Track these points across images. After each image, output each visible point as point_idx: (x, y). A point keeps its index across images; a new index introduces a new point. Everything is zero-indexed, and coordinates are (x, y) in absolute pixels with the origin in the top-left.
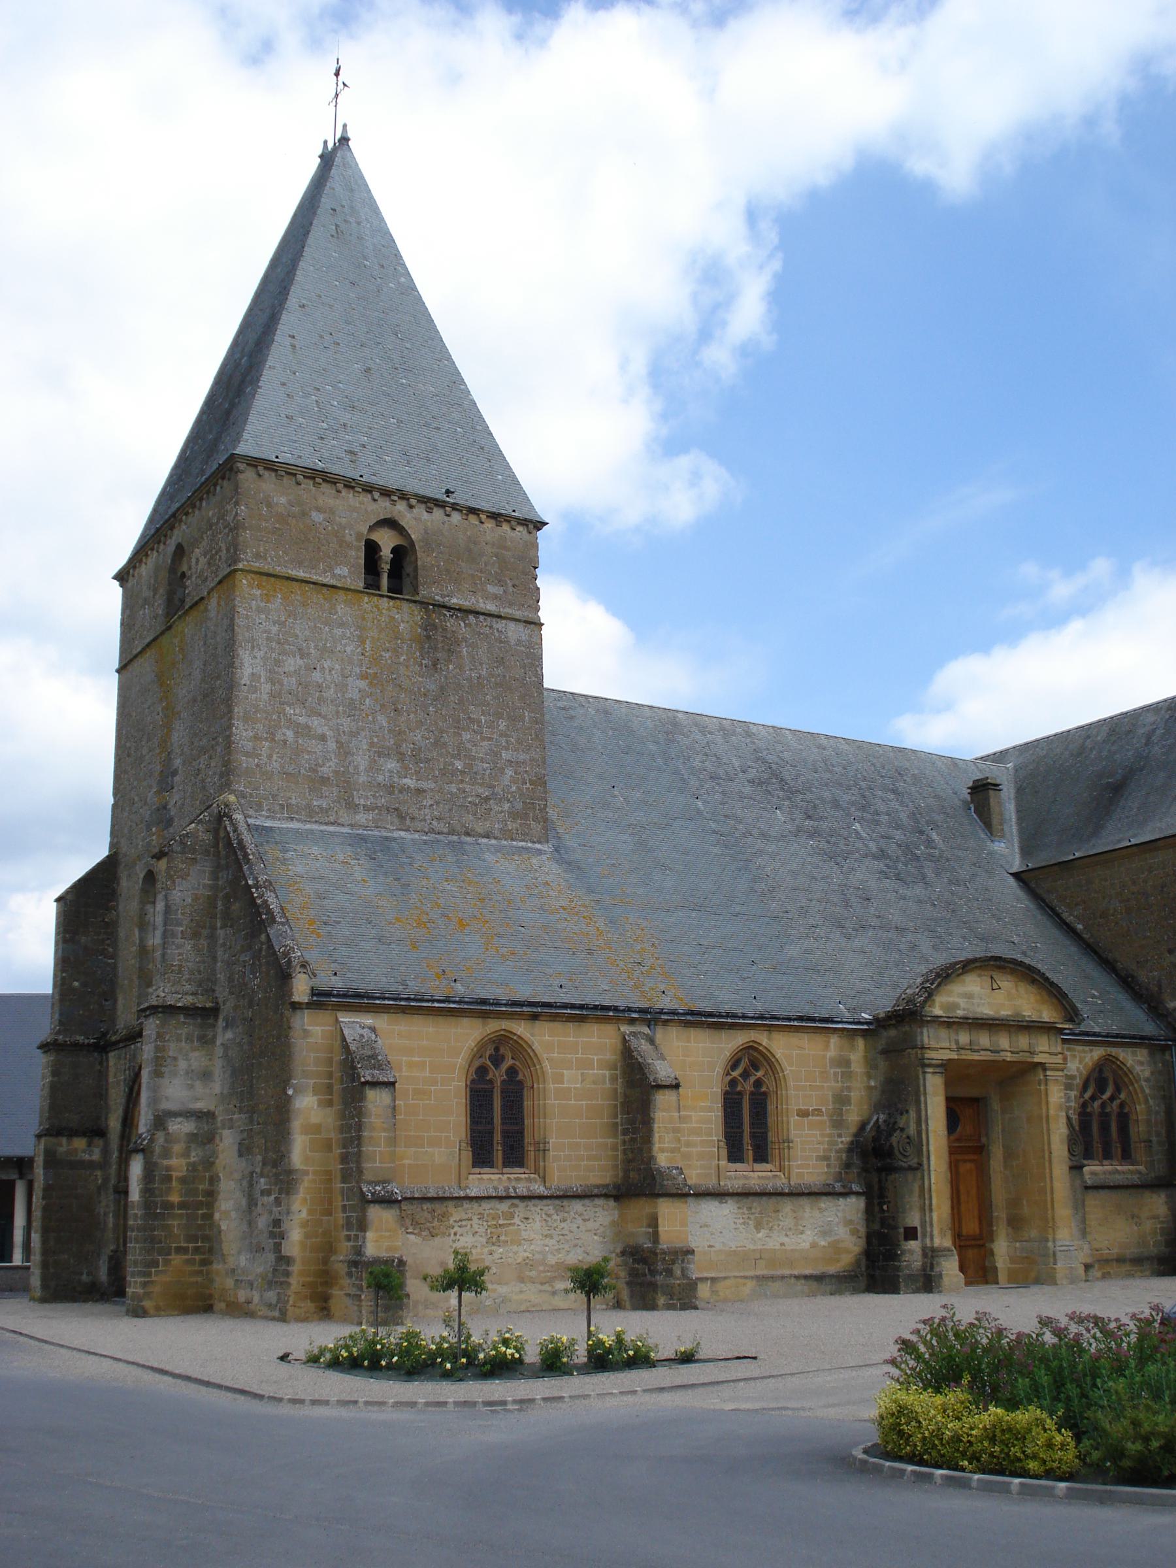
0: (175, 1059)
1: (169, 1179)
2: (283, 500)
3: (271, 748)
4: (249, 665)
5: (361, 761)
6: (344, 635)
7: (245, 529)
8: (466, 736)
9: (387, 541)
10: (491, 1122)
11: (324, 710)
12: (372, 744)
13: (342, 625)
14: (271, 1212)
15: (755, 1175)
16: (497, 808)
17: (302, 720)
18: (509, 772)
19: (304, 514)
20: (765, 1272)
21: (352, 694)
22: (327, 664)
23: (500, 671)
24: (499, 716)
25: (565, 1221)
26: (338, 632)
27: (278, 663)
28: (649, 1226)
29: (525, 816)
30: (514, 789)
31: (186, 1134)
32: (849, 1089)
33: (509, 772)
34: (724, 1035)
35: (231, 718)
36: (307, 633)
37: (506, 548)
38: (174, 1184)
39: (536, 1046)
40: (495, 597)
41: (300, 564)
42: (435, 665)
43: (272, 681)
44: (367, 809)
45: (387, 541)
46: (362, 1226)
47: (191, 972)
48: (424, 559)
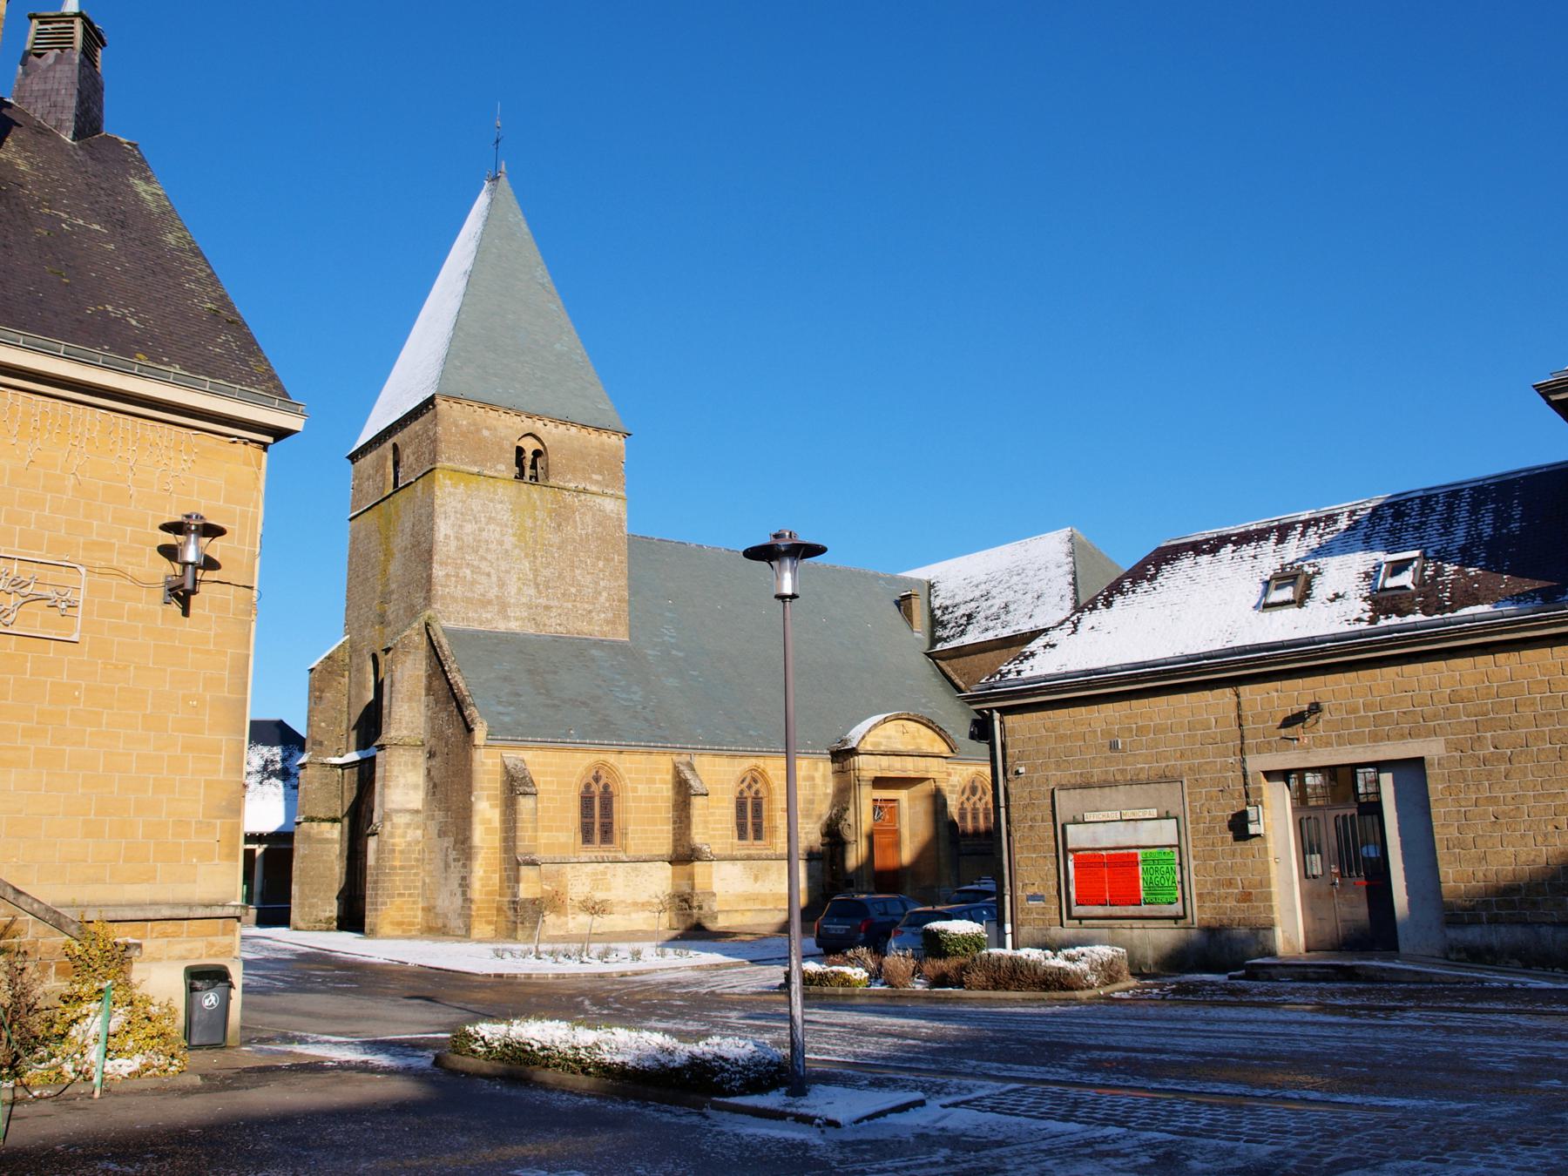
1: (393, 851)
2: (464, 423)
4: (443, 529)
8: (578, 572)
9: (530, 445)
10: (593, 817)
11: (489, 557)
12: (519, 579)
13: (501, 502)
14: (460, 872)
15: (751, 846)
16: (596, 618)
17: (476, 563)
18: (605, 594)
19: (478, 431)
20: (760, 907)
21: (508, 546)
22: (492, 527)
23: (600, 529)
24: (598, 559)
25: (637, 876)
26: (499, 506)
27: (461, 526)
28: (689, 879)
29: (614, 623)
30: (607, 605)
33: (605, 594)
34: (737, 761)
35: (431, 563)
36: (479, 507)
37: (604, 450)
39: (621, 770)
40: (597, 482)
41: (475, 463)
43: (457, 539)
44: (516, 619)
45: (530, 445)
46: (517, 880)
47: (407, 723)
48: (553, 458)
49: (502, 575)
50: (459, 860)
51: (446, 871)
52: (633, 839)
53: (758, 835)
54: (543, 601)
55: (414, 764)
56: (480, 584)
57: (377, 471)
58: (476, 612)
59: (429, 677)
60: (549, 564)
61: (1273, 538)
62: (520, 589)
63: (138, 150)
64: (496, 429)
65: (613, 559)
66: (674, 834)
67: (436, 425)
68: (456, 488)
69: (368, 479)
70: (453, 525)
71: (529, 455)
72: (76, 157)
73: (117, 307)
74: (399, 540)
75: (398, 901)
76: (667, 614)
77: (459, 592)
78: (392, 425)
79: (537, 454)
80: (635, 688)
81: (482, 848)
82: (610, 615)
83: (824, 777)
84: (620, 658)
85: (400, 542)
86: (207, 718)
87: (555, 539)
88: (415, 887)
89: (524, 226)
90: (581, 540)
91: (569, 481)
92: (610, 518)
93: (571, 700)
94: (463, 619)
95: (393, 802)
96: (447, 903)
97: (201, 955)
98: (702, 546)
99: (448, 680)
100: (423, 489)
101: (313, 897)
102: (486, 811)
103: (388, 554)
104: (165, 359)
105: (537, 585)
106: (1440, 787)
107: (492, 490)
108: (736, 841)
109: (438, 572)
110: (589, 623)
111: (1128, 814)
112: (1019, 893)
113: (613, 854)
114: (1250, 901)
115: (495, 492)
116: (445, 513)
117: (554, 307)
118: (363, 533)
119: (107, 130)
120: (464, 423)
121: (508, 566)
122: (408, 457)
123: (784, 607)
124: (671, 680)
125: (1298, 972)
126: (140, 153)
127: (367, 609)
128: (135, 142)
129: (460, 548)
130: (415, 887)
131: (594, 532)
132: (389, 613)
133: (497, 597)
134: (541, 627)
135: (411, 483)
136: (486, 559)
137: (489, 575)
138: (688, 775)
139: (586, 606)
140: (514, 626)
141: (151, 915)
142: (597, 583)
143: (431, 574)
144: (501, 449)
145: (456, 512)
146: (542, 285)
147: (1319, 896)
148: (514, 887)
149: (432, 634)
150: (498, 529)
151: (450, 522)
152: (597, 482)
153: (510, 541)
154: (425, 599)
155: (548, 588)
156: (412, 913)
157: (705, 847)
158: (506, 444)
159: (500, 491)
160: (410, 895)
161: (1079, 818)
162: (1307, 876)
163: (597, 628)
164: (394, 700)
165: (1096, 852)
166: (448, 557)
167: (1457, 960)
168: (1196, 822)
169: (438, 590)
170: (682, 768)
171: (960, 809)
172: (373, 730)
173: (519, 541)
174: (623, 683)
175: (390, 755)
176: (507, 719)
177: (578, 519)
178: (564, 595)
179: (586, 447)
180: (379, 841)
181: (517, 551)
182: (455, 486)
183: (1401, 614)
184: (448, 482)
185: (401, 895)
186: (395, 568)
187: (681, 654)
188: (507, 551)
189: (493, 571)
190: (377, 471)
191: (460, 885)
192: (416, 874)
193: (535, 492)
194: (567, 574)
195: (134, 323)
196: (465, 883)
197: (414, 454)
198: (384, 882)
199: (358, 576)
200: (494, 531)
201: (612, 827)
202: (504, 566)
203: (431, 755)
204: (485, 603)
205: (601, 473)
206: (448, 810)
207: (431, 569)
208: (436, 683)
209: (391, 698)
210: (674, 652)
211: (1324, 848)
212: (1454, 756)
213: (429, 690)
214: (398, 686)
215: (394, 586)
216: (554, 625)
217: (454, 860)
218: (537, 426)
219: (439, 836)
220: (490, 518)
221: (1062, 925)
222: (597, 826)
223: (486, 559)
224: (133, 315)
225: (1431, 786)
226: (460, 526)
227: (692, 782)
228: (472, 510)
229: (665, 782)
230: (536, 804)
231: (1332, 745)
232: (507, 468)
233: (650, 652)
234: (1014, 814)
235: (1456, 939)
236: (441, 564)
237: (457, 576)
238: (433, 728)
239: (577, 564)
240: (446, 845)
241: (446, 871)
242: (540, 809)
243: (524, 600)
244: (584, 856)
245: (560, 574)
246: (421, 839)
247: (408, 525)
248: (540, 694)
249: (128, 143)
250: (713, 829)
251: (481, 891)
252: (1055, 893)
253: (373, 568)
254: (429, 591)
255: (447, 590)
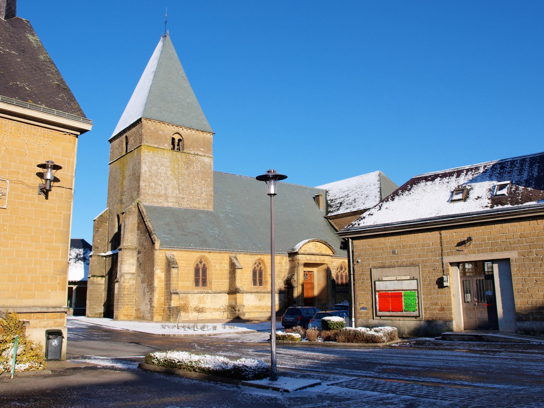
0: (126, 261)
2: (153, 128)
3: (149, 188)
4: (144, 168)
5: (170, 191)
6: (166, 161)
7: (144, 135)
8: (195, 185)
9: (177, 137)
11: (161, 179)
12: (173, 187)
13: (166, 158)
14: (149, 296)
15: (258, 288)
16: (201, 202)
17: (156, 181)
18: (204, 193)
19: (158, 131)
21: (168, 175)
22: (162, 168)
23: (203, 169)
24: (202, 180)
25: (215, 298)
26: (165, 160)
28: (235, 300)
30: (205, 197)
31: (129, 278)
32: (282, 269)
33: (204, 193)
34: (253, 256)
35: (139, 181)
38: (126, 289)
39: (210, 259)
41: (156, 143)
42: (188, 168)
43: (150, 172)
44: (171, 202)
45: (177, 137)
46: (171, 300)
48: (186, 142)
49: (166, 186)
50: (149, 292)
51: (144, 296)
52: (214, 284)
53: (261, 284)
54: (181, 196)
55: (132, 256)
56: (158, 189)
57: (120, 146)
58: (156, 199)
59: (139, 223)
60: (184, 182)
61: (455, 175)
62: (173, 191)
63: (29, 23)
64: (164, 131)
65: (208, 180)
66: (229, 283)
67: (142, 129)
68: (149, 153)
69: (116, 149)
70: (148, 167)
71: (176, 141)
72: (6, 26)
73: (21, 83)
74: (128, 172)
75: (126, 307)
76: (228, 201)
77: (150, 192)
78: (125, 129)
79: (180, 140)
80: (215, 229)
81: (158, 287)
82: (207, 201)
83: (286, 262)
84: (210, 217)
85: (128, 173)
86: (54, 237)
87: (186, 172)
88: (133, 302)
89: (176, 54)
90: (196, 173)
91: (192, 151)
92: (207, 165)
93: (191, 232)
94: (151, 202)
95: (124, 270)
96: (144, 308)
97: (52, 326)
98: (241, 176)
99: (145, 225)
100: (137, 153)
101: (94, 305)
102: (159, 274)
103: (123, 177)
104: (39, 103)
105: (179, 190)
106: (516, 269)
107: (163, 153)
108: (252, 286)
109: (142, 184)
110: (199, 204)
111: (399, 278)
112: (358, 307)
113: (207, 290)
114: (444, 311)
115: (164, 155)
116: (145, 162)
117: (186, 85)
118: (114, 170)
119: (17, 16)
120: (153, 128)
121: (168, 182)
122: (131, 141)
123: (271, 198)
124: (229, 226)
125: (461, 337)
126: (30, 25)
127: (115, 198)
128: (28, 20)
129: (150, 175)
130: (133, 302)
131: (201, 170)
132: (124, 199)
133: (164, 194)
134: (181, 205)
135: (132, 151)
136: (160, 180)
137: (161, 185)
138: (235, 261)
139: (198, 198)
140: (170, 205)
141: (33, 311)
142: (201, 189)
143: (139, 185)
144: (166, 138)
145: (149, 162)
146: (182, 77)
147: (470, 309)
148: (169, 302)
149: (140, 207)
150: (165, 168)
151: (147, 166)
152: (202, 151)
153: (169, 173)
154: (137, 194)
155: (183, 191)
156: (131, 311)
157: (241, 288)
158: (168, 137)
159: (166, 154)
160: (131, 305)
161: (380, 279)
162: (465, 302)
163: (201, 206)
164: (125, 232)
165: (387, 292)
166: (146, 179)
167: (520, 334)
168: (424, 281)
169: (142, 191)
170: (233, 258)
171: (336, 275)
172: (117, 243)
173: (173, 173)
174: (211, 227)
175: (124, 253)
176: (167, 239)
177: (195, 165)
178: (189, 193)
179: (198, 138)
180: (119, 284)
181: (172, 177)
182: (149, 152)
183: (502, 204)
184: (146, 150)
185: (127, 305)
186: (126, 182)
187: (233, 216)
188: (168, 176)
189: (162, 184)
190: (120, 146)
191: (149, 301)
192: (132, 297)
193: (179, 154)
194: (190, 185)
195: (28, 89)
196: (151, 301)
197: (133, 140)
198: (121, 300)
199: (112, 186)
200: (163, 169)
201: (206, 280)
202: (167, 182)
203: (139, 253)
204: (160, 196)
205: (203, 148)
206: (145, 273)
207: (139, 183)
208: (141, 226)
209: (124, 231)
210: (230, 215)
211: (472, 292)
212: (521, 258)
213: (138, 228)
214: (127, 226)
215: (125, 189)
216: (185, 205)
217: (147, 292)
218: (180, 130)
219: (142, 283)
220: (162, 164)
221: (373, 319)
222: (201, 280)
223: (160, 180)
224: (27, 86)
225: (512, 269)
226: (151, 167)
227: (236, 264)
228: (155, 161)
229: (226, 264)
230: (178, 271)
231: (475, 253)
232: (168, 145)
233: (221, 215)
234: (356, 277)
235: (520, 326)
236: (143, 181)
237: (149, 186)
238: (140, 242)
239: (194, 182)
240: (144, 286)
241: (144, 296)
242: (179, 273)
243: (174, 195)
244: (196, 291)
245: (188, 186)
246: (135, 284)
247: (131, 166)
248: (180, 230)
249: (26, 21)
250: (244, 282)
251: (157, 303)
252: (371, 307)
253: (118, 182)
254: (139, 191)
255: (146, 191)
